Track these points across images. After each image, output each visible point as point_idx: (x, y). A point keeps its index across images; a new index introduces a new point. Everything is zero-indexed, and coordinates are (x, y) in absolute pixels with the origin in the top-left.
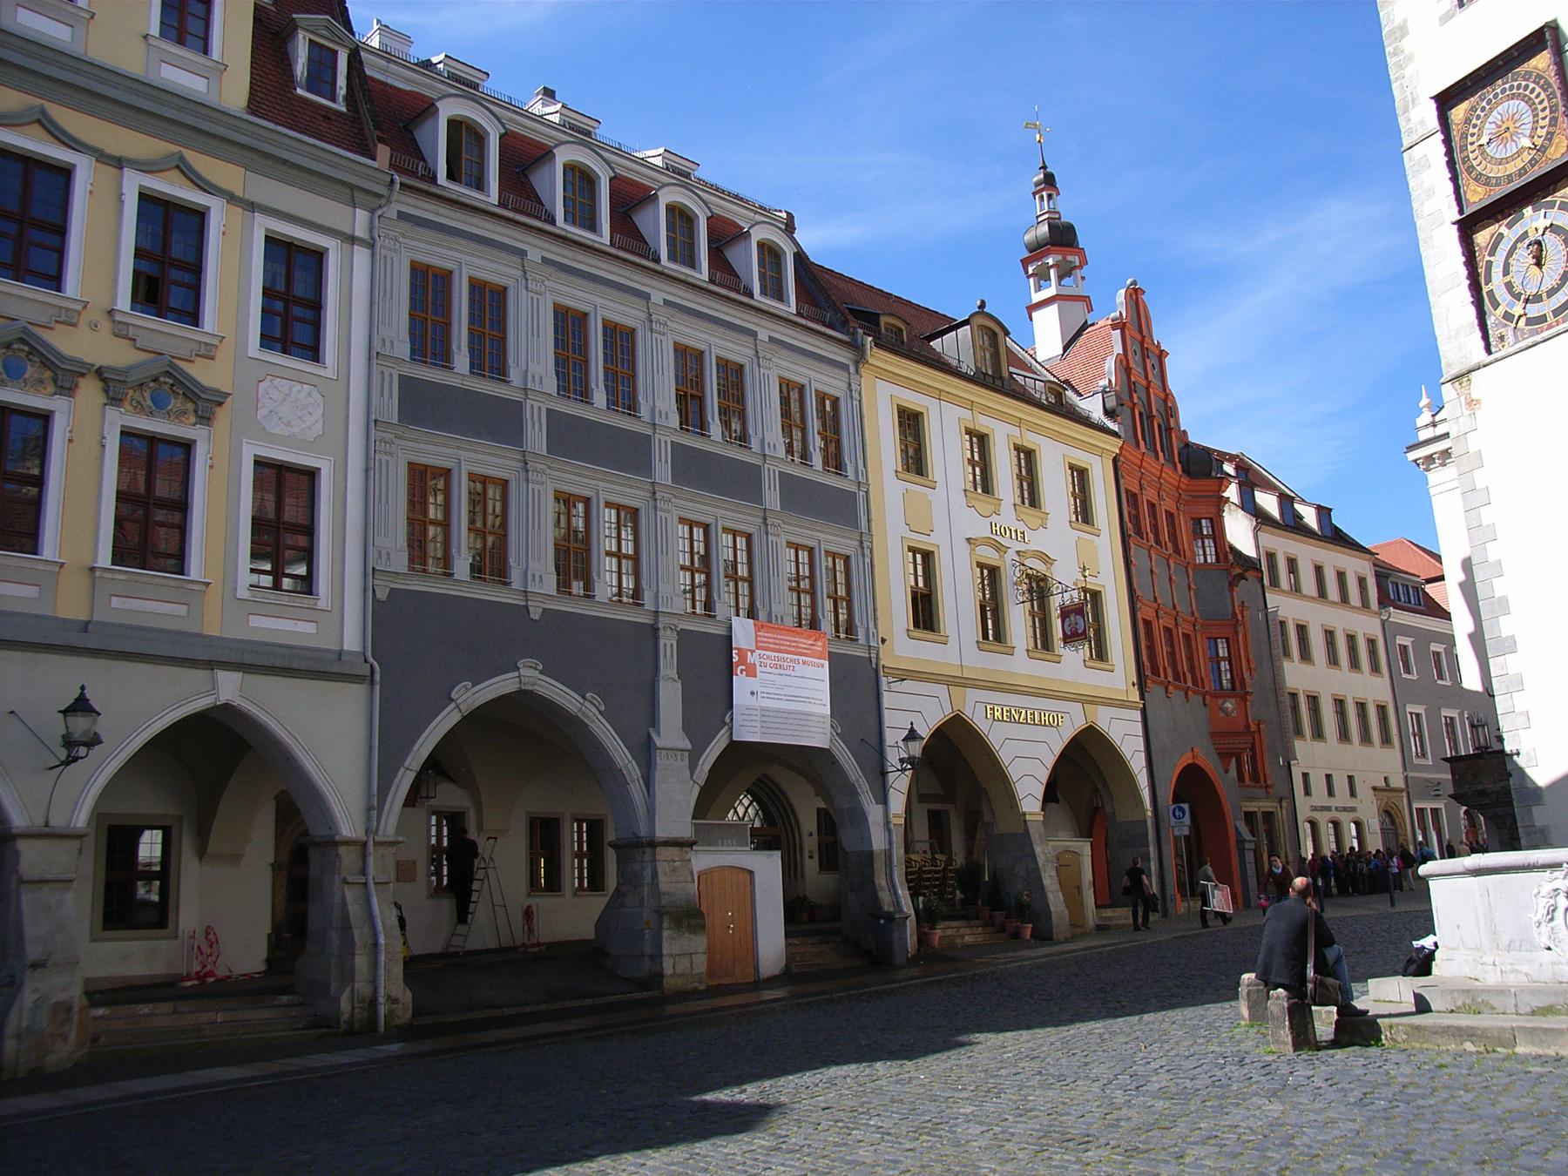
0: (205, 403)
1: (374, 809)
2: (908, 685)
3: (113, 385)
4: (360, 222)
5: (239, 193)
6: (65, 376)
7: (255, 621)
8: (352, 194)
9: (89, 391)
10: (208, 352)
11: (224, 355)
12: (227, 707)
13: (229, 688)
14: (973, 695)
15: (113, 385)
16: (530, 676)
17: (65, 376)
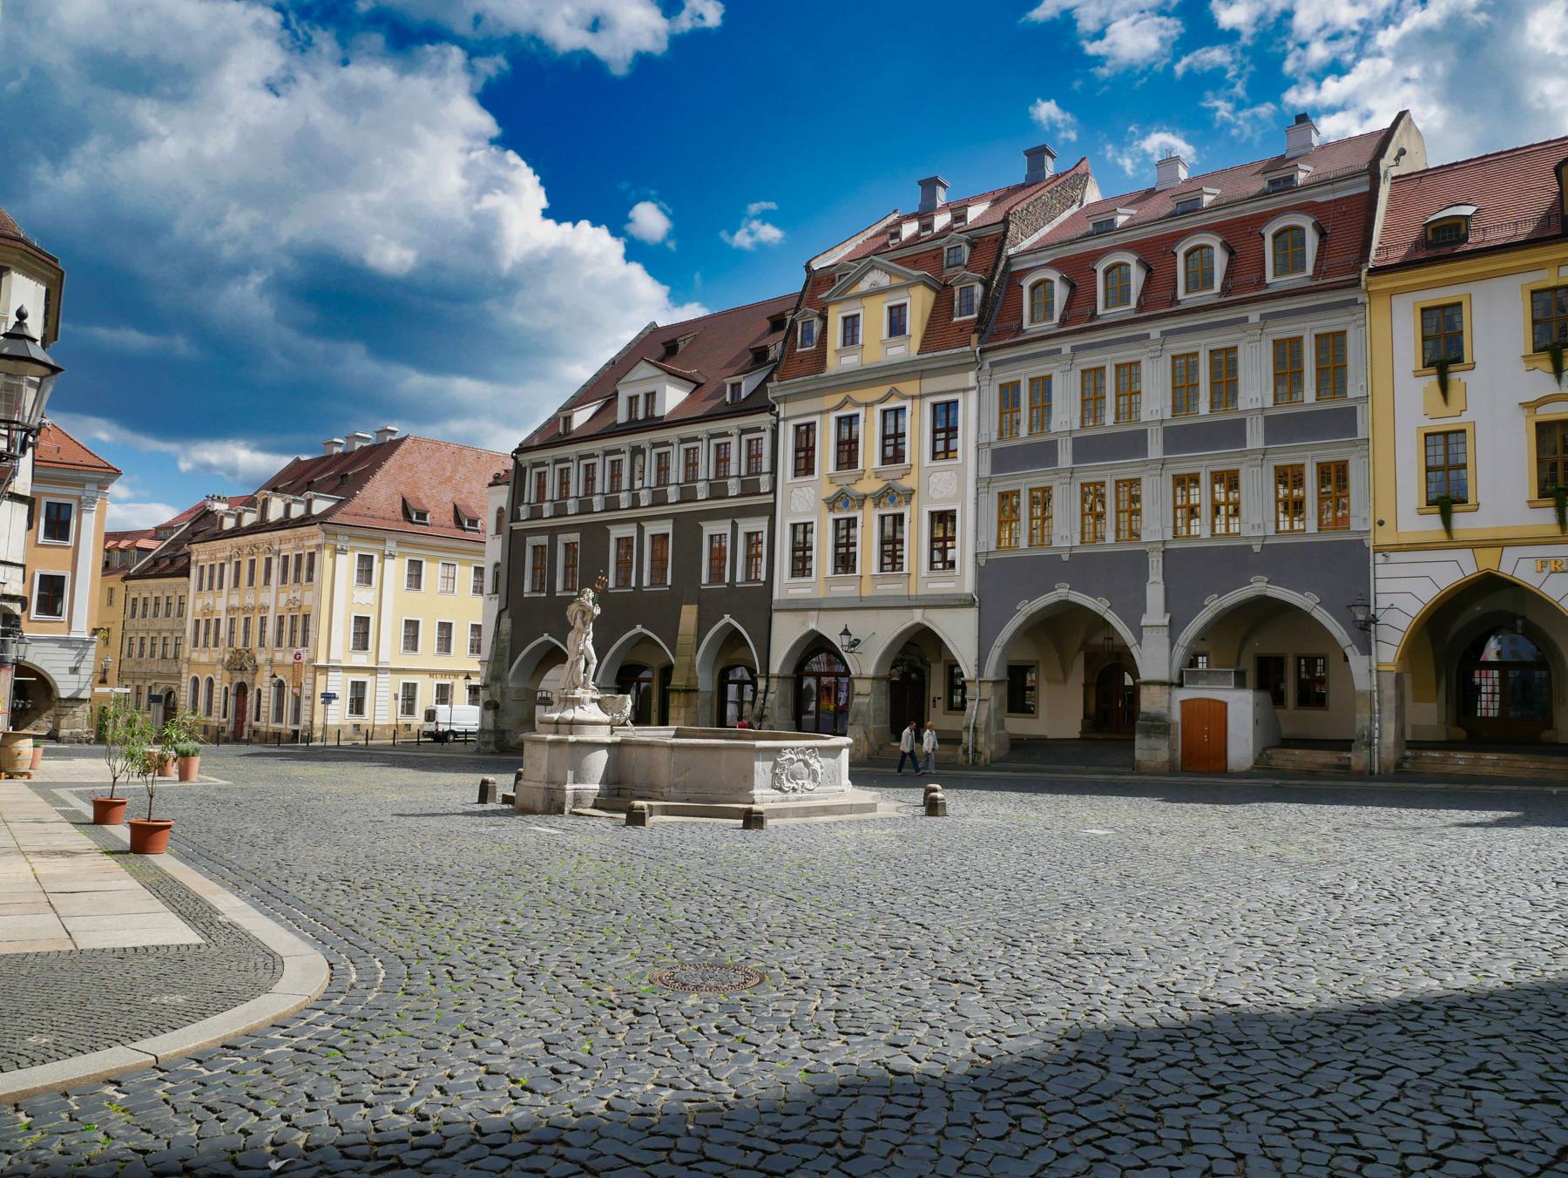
0: (909, 494)
1: (980, 666)
2: (1394, 557)
3: (878, 498)
4: (970, 378)
5: (917, 392)
6: (861, 501)
7: (931, 586)
8: (963, 367)
9: (869, 504)
10: (907, 472)
11: (914, 471)
12: (918, 624)
13: (917, 616)
14: (1510, 554)
15: (878, 498)
16: (1062, 592)
17: (861, 501)
